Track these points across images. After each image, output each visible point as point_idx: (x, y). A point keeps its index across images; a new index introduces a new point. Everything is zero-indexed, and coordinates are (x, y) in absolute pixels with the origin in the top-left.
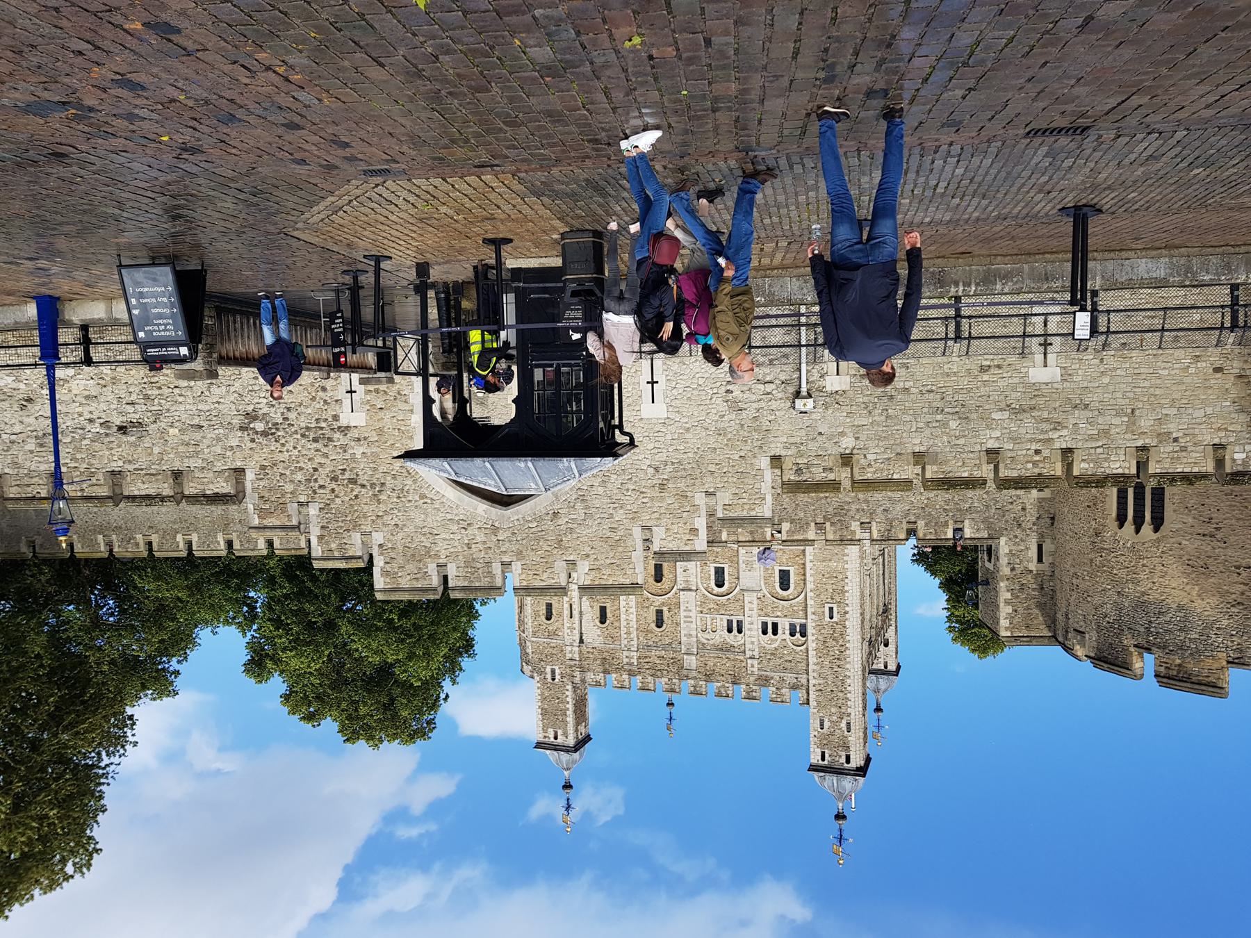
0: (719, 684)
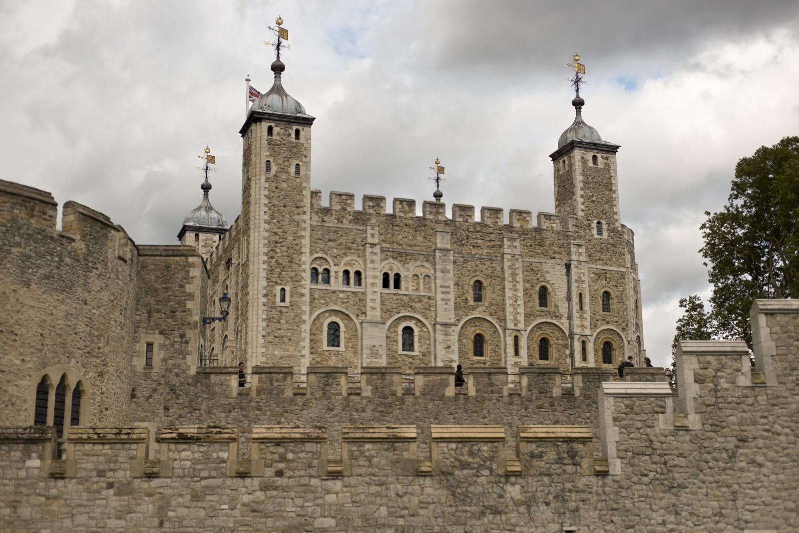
0: (410, 215)
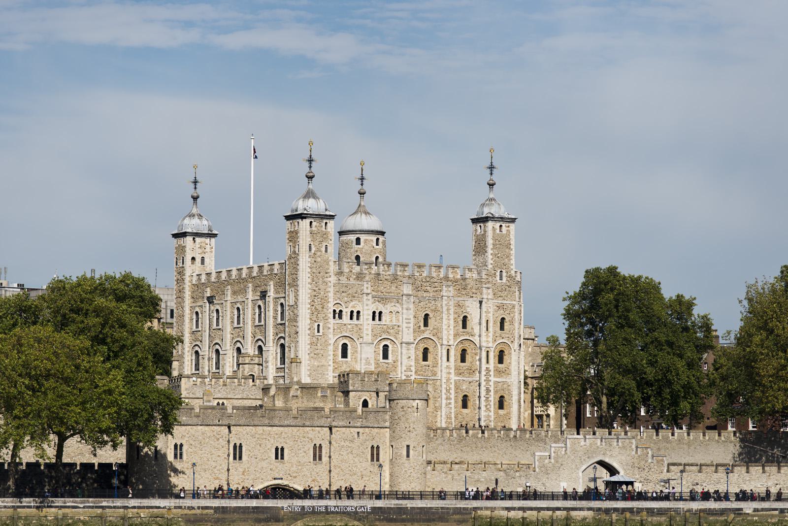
0: (388, 273)
